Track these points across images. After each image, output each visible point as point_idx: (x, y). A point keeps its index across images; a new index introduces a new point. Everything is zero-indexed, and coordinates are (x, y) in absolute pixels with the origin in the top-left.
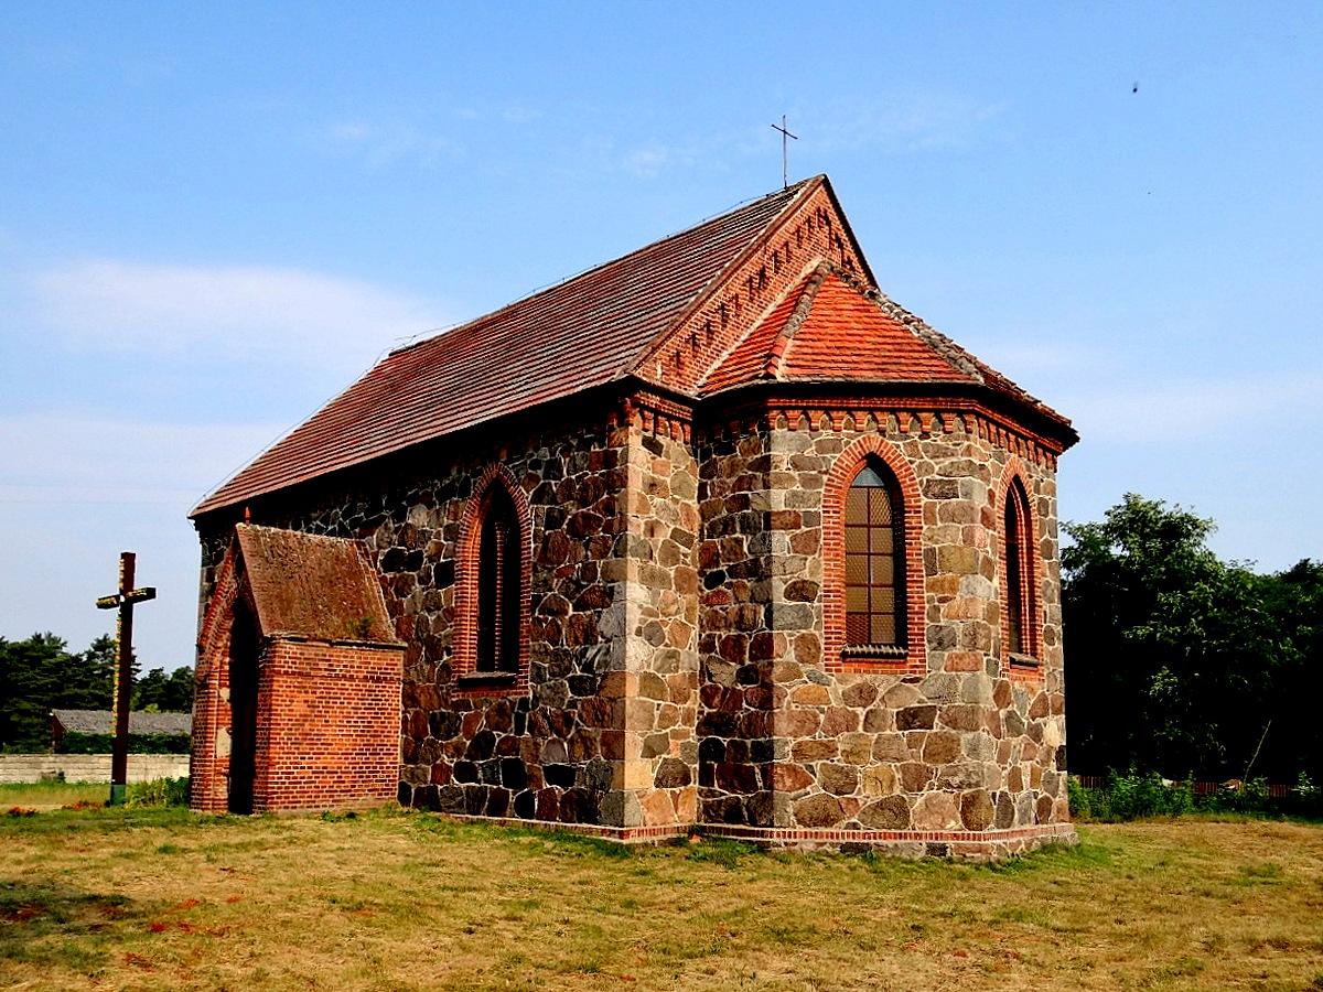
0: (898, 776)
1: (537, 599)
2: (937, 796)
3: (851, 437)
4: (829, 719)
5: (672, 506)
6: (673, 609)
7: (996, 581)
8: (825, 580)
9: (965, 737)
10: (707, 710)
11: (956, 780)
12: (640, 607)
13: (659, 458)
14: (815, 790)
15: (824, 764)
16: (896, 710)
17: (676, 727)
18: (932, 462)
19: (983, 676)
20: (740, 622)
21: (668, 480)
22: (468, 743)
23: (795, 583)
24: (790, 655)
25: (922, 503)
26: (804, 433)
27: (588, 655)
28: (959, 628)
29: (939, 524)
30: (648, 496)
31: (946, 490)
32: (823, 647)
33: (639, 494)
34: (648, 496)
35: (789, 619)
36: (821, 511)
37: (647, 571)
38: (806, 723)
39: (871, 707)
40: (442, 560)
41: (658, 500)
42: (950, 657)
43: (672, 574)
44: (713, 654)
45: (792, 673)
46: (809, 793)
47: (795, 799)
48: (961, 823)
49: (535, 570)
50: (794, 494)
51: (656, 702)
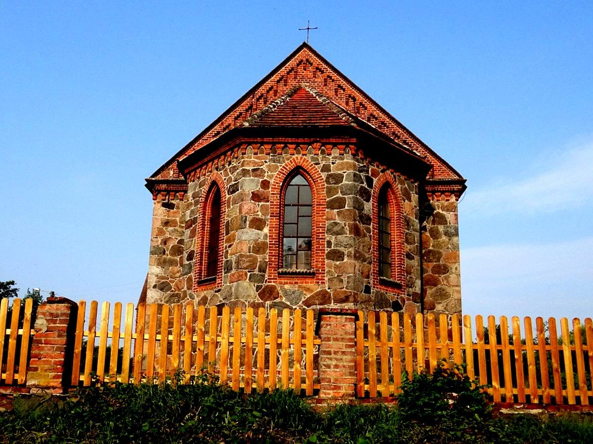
5: (180, 229)
6: (178, 275)
7: (266, 230)
12: (157, 276)
19: (246, 283)
21: (178, 219)
28: (234, 259)
30: (164, 228)
31: (234, 189)
33: (158, 228)
34: (164, 228)
37: (162, 260)
41: (170, 229)
43: (178, 259)
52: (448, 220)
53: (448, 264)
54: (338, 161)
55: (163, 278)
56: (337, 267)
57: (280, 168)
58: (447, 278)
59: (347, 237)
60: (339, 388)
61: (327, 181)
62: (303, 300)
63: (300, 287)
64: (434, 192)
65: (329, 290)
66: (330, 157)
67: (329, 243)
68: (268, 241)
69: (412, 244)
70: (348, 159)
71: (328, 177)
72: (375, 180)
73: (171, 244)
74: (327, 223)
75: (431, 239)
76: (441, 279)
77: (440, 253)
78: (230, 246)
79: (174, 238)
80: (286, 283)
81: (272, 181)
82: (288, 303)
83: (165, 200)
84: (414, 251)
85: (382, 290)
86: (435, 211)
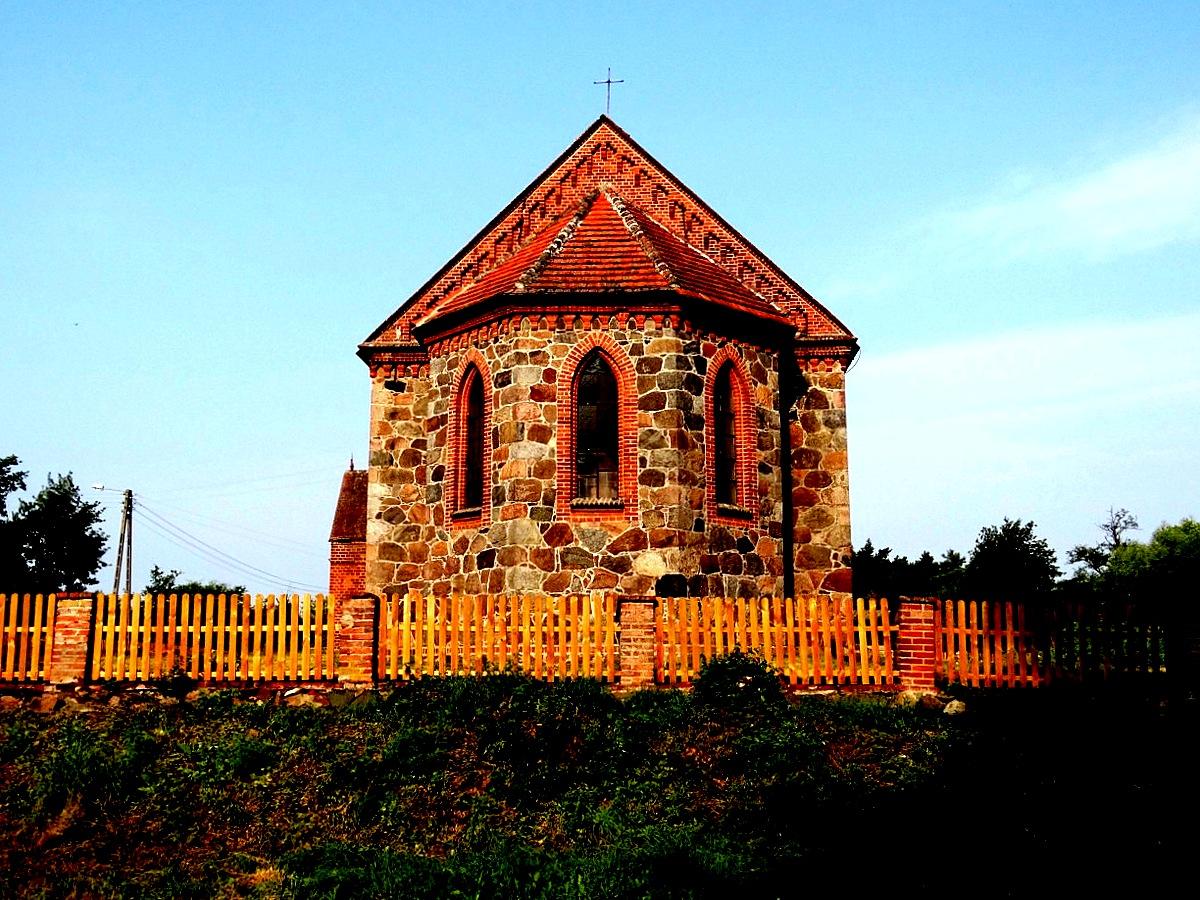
4: (448, 565)
5: (414, 424)
6: (414, 496)
7: (553, 443)
9: (509, 571)
12: (381, 499)
13: (401, 394)
17: (417, 580)
19: (525, 521)
21: (411, 408)
28: (507, 485)
30: (390, 423)
31: (504, 380)
33: (380, 422)
34: (390, 423)
37: (388, 474)
41: (399, 423)
43: (414, 472)
51: (396, 563)
52: (830, 401)
53: (829, 470)
54: (654, 339)
55: (390, 502)
56: (654, 495)
57: (572, 349)
58: (828, 493)
59: (667, 451)
60: (639, 674)
61: (639, 370)
62: (608, 543)
63: (602, 525)
64: (807, 358)
65: (644, 530)
66: (643, 333)
67: (643, 461)
68: (556, 459)
69: (768, 449)
70: (669, 336)
71: (640, 362)
72: (709, 361)
73: (401, 449)
74: (640, 431)
75: (805, 432)
76: (819, 494)
77: (818, 455)
78: (501, 466)
79: (405, 437)
80: (582, 521)
81: (559, 370)
82: (587, 549)
83: (389, 377)
84: (772, 459)
85: (722, 523)
86: (810, 388)
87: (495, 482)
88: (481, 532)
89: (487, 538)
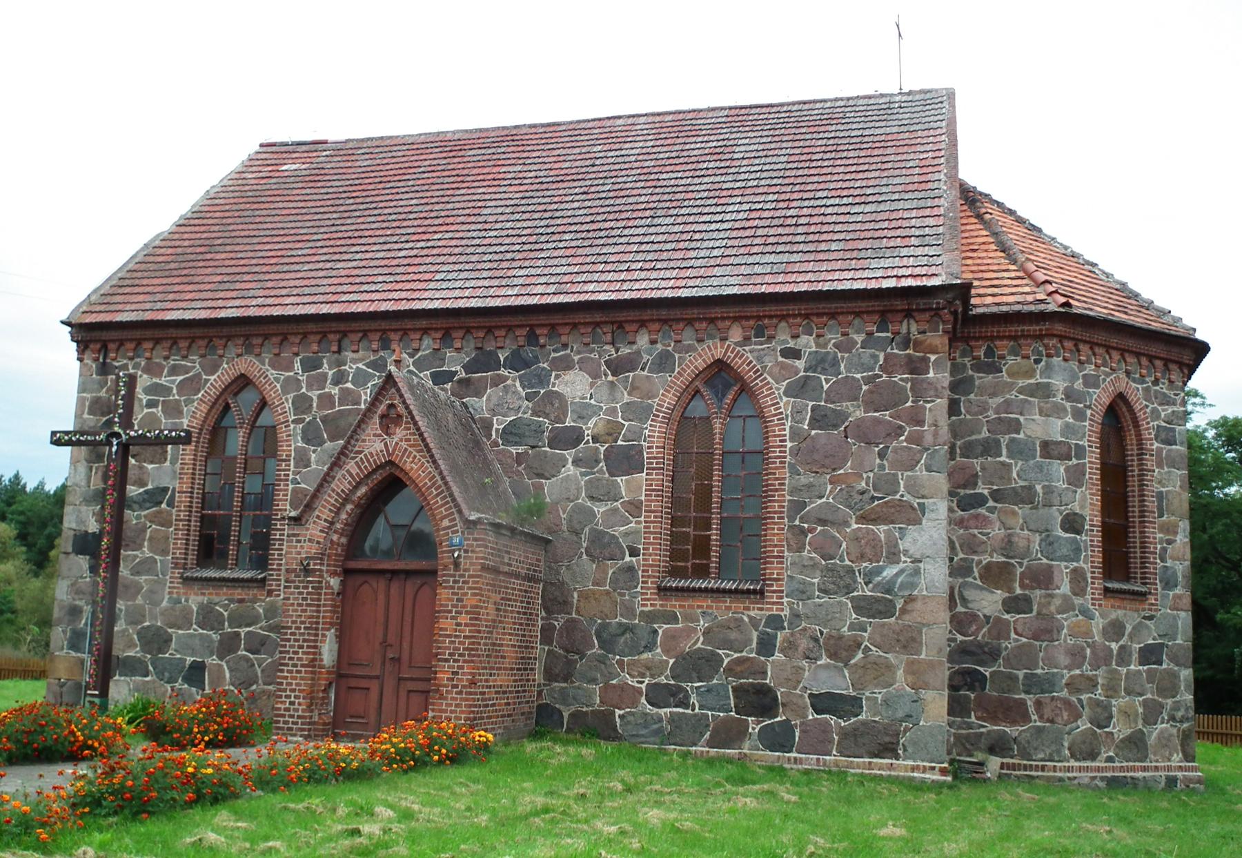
0: (1141, 710)
1: (798, 506)
2: (1166, 728)
3: (1108, 375)
8: (1090, 515)
10: (960, 638)
11: (1179, 714)
14: (1084, 725)
15: (1090, 698)
16: (1138, 646)
18: (1159, 408)
20: (1008, 546)
22: (672, 661)
23: (1067, 514)
24: (1065, 588)
25: (1154, 447)
26: (1074, 365)
27: (885, 574)
29: (1166, 469)
32: (1090, 580)
35: (1065, 551)
36: (1086, 444)
38: (1076, 656)
39: (1121, 643)
40: (620, 443)
42: (1174, 597)
44: (970, 579)
45: (1067, 607)
46: (1079, 727)
47: (1069, 733)
48: (1181, 755)
49: (794, 472)
50: (1067, 425)
78: (1169, 542)
87: (1163, 560)
88: (1144, 618)
89: (1152, 626)
